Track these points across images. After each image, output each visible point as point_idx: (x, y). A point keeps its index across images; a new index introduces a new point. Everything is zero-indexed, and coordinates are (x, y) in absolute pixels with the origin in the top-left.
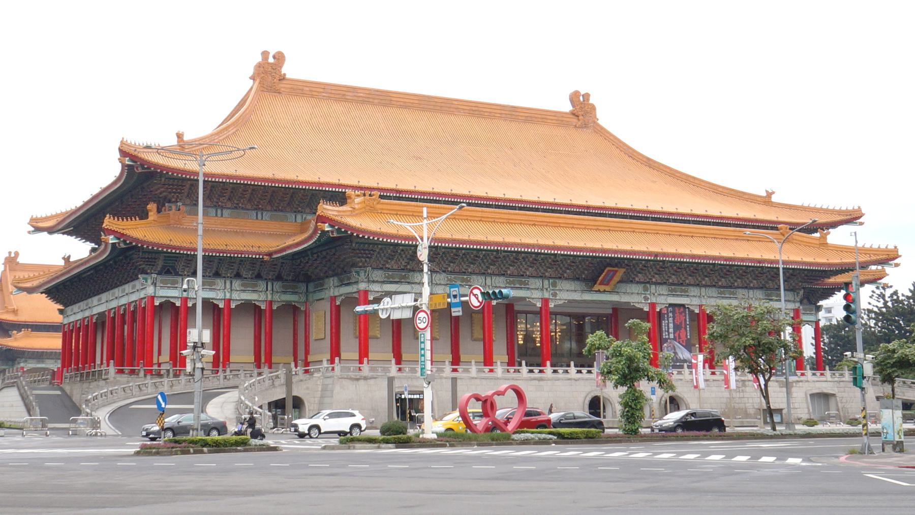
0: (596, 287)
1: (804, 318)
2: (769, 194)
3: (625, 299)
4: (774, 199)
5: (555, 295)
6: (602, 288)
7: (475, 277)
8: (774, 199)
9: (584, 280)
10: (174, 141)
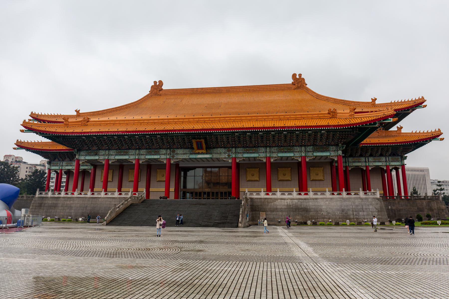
3: (215, 156)
4: (377, 102)
5: (173, 156)
6: (200, 151)
8: (377, 102)
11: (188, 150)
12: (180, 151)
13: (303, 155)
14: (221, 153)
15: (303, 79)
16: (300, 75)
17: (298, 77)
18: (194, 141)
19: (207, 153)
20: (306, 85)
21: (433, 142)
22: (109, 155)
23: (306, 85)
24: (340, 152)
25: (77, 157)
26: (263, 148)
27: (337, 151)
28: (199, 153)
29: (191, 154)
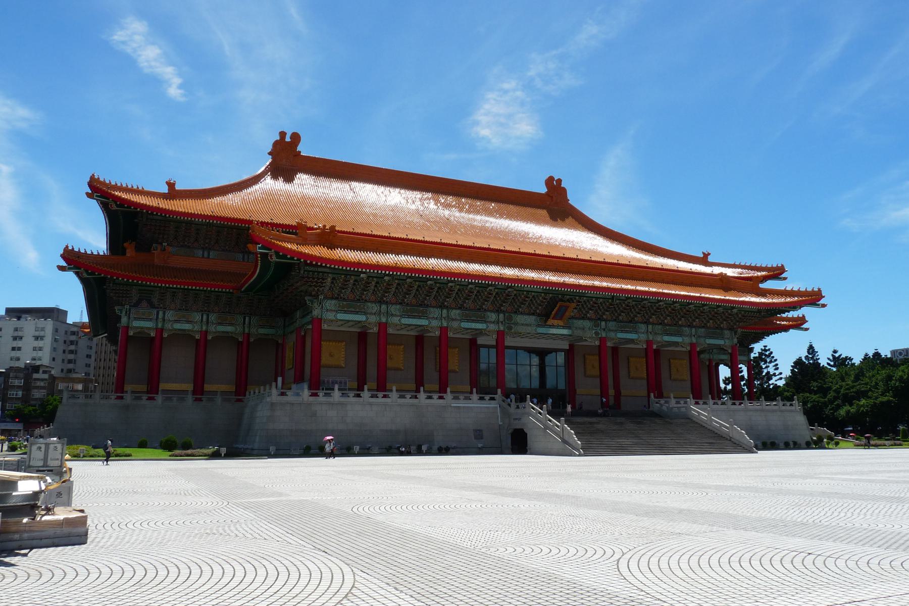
0: (551, 322)
1: (740, 358)
2: (706, 255)
3: (579, 333)
5: (510, 328)
6: (556, 322)
7: (432, 309)
8: (710, 259)
9: (539, 315)
10: (165, 189)
11: (533, 318)
12: (520, 319)
13: (694, 341)
15: (564, 190)
16: (559, 181)
19: (564, 327)
21: (792, 331)
22: (388, 314)
24: (735, 341)
25: (316, 313)
27: (733, 339)
28: (553, 326)
29: (539, 326)
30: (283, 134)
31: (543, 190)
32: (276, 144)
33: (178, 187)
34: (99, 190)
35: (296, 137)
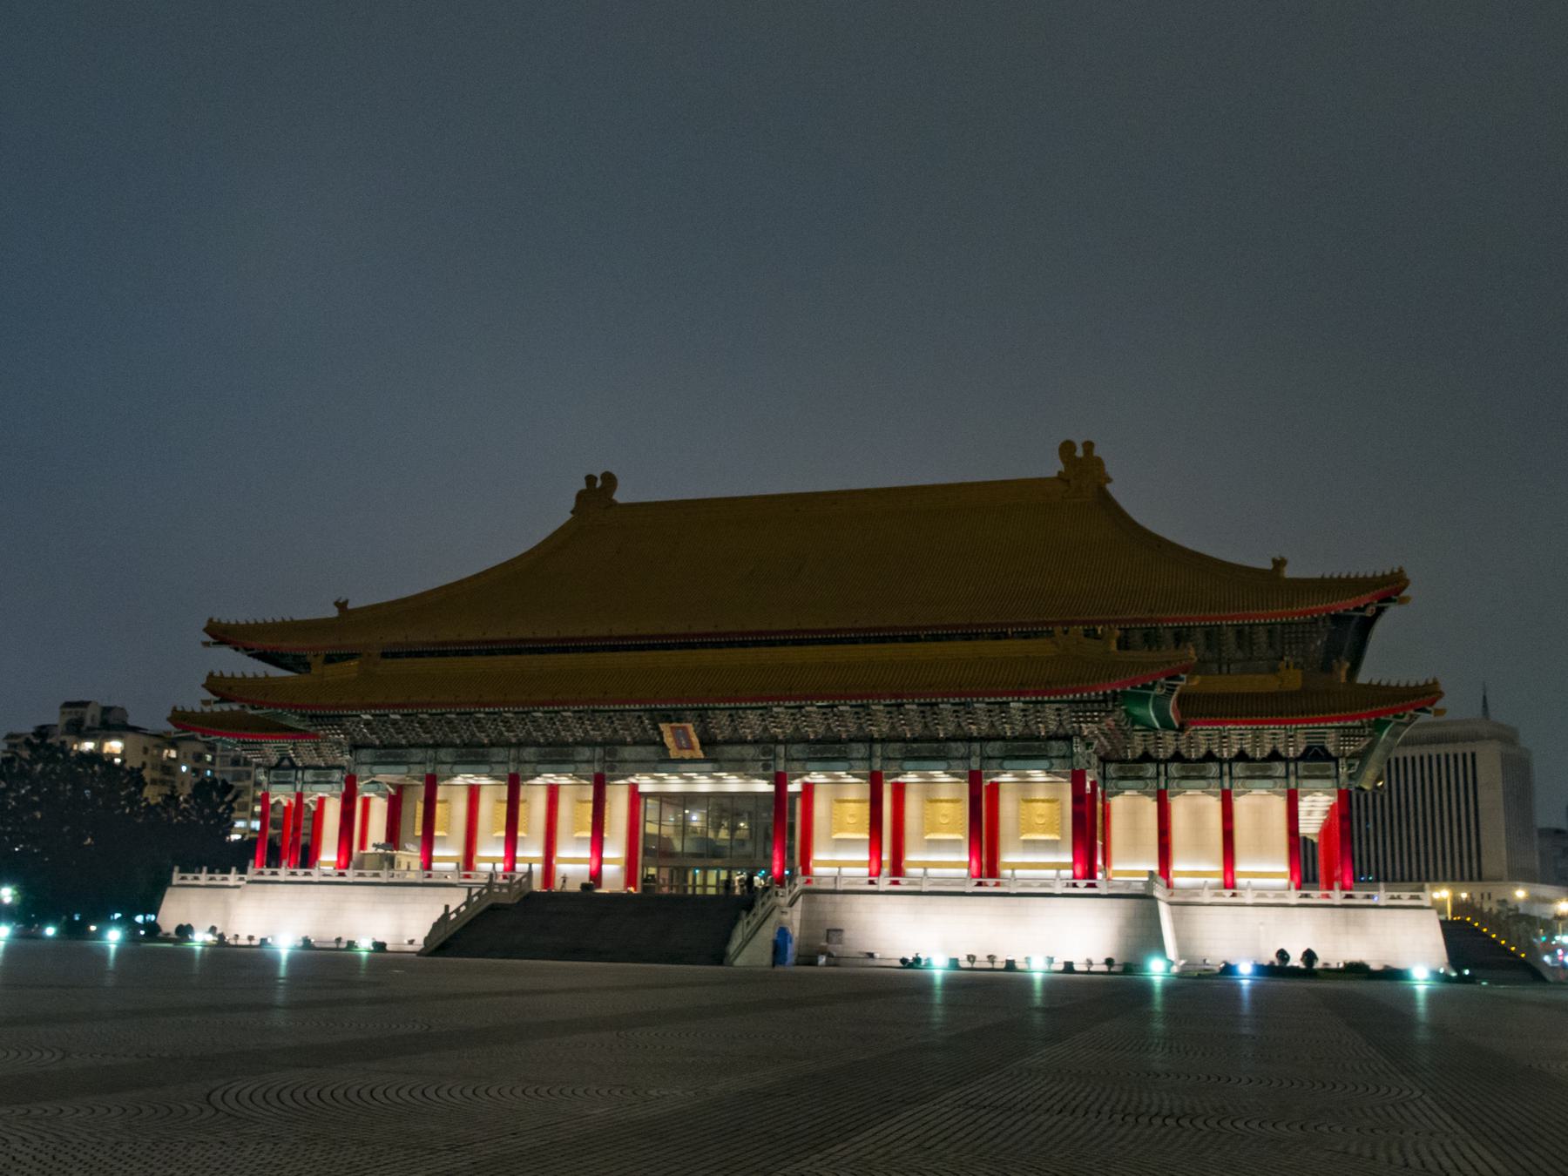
2: (1279, 564)
10: (333, 613)
14: (744, 760)
16: (1088, 446)
17: (1080, 453)
18: (663, 726)
20: (1109, 480)
23: (1109, 480)
26: (860, 745)
30: (590, 479)
31: (1052, 467)
32: (580, 496)
33: (350, 606)
34: (221, 634)
35: (610, 479)
